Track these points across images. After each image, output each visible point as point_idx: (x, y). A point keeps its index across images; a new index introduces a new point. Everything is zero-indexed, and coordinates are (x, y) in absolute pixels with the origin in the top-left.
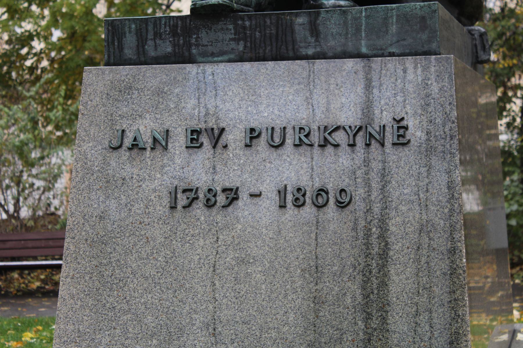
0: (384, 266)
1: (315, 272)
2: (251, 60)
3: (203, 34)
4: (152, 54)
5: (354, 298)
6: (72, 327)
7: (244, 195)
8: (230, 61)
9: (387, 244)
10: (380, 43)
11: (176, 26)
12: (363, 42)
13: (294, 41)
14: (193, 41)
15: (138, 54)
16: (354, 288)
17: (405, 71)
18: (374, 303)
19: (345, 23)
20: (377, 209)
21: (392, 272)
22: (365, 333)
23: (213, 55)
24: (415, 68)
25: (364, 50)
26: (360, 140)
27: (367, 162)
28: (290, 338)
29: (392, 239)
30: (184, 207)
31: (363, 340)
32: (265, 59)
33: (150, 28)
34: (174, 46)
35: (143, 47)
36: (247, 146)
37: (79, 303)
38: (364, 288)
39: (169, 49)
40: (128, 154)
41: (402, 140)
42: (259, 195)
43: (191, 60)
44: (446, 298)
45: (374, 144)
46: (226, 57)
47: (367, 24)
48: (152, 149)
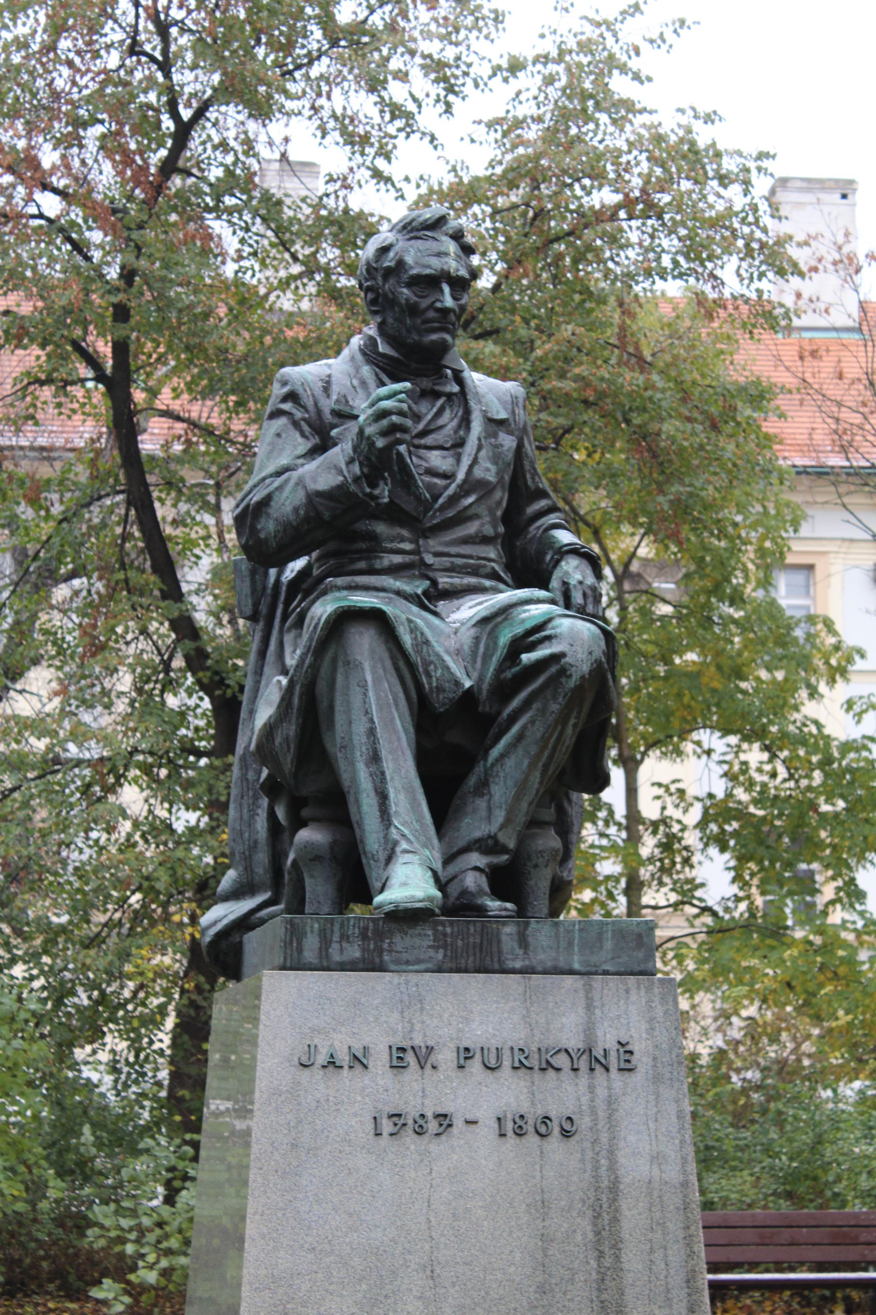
0: (615, 1200)
1: (542, 1206)
2: (451, 971)
3: (397, 939)
4: (337, 958)
5: (584, 1235)
6: (264, 1272)
7: (458, 1123)
8: (427, 971)
9: (616, 1178)
10: (594, 959)
11: (366, 929)
12: (576, 958)
13: (500, 952)
14: (386, 946)
15: (320, 958)
16: (585, 1225)
17: (627, 991)
18: (606, 1239)
19: (557, 935)
20: (604, 1138)
21: (624, 1206)
22: (599, 1272)
23: (408, 962)
24: (638, 988)
25: (576, 966)
26: (583, 1064)
27: (591, 1089)
28: (517, 1279)
29: (621, 1172)
30: (391, 1135)
31: (596, 1281)
32: (466, 971)
33: (336, 928)
34: (363, 950)
35: (327, 949)
36: (461, 1067)
37: (272, 1244)
38: (595, 1225)
39: (357, 954)
40: (321, 1072)
41: (628, 1066)
42: (476, 1122)
43: (381, 968)
44: (681, 1234)
45: (599, 1069)
46: (422, 967)
47: (581, 937)
48: (351, 1067)
